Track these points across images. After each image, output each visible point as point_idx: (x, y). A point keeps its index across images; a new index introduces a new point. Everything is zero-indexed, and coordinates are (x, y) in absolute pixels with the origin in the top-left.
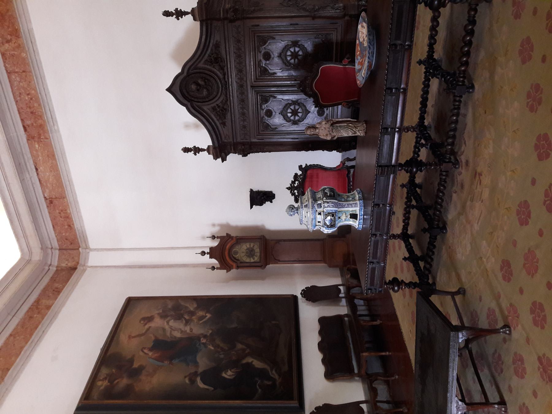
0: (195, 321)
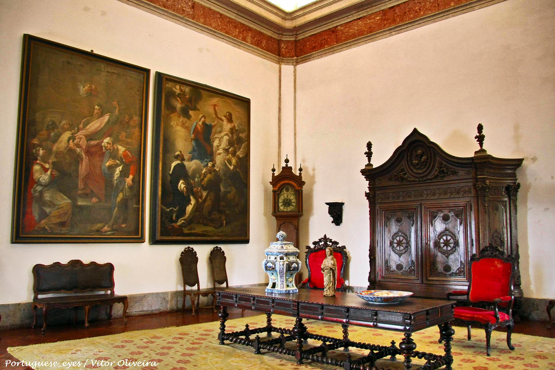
0: (228, 157)
